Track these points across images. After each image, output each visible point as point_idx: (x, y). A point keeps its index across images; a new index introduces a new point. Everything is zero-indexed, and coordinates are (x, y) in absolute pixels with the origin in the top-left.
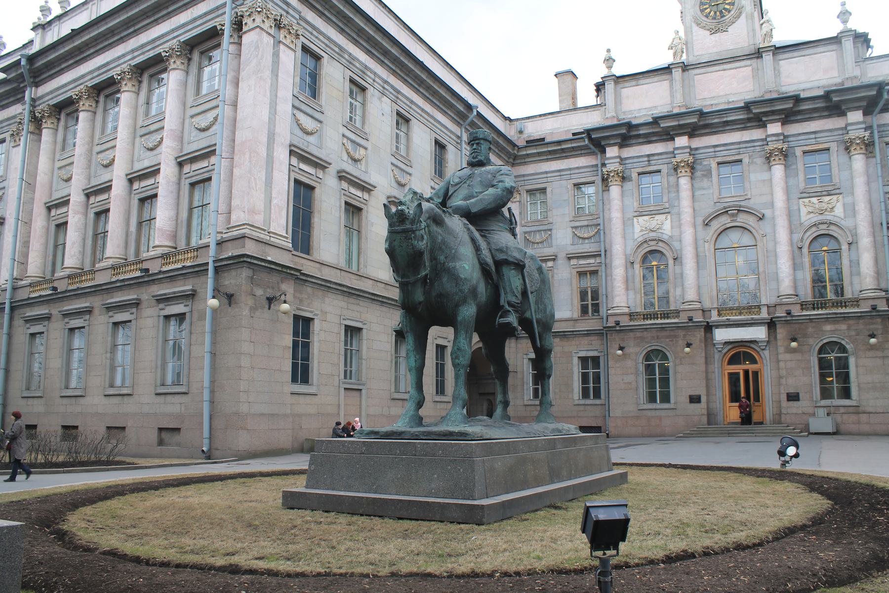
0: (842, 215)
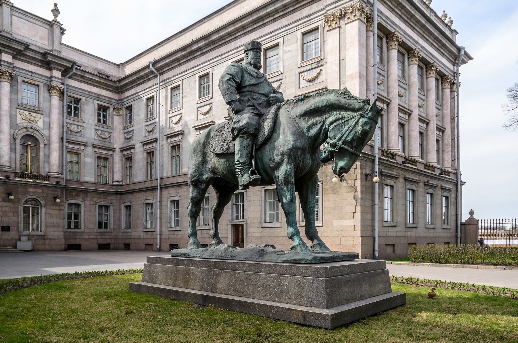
0: (42, 127)
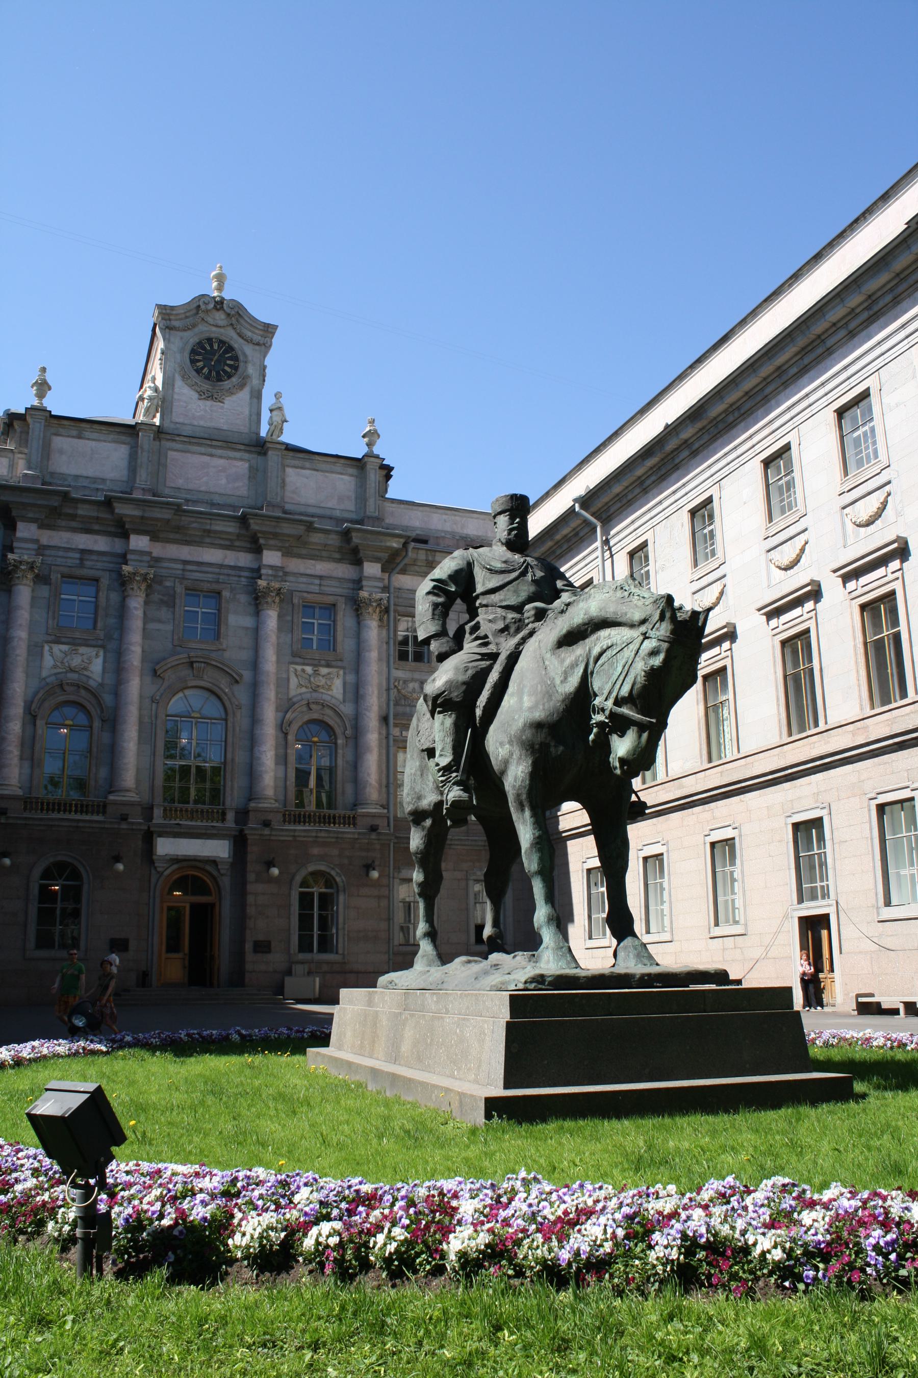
0: (340, 697)
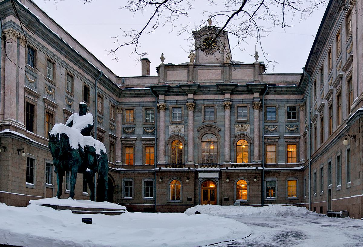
0: (249, 132)
